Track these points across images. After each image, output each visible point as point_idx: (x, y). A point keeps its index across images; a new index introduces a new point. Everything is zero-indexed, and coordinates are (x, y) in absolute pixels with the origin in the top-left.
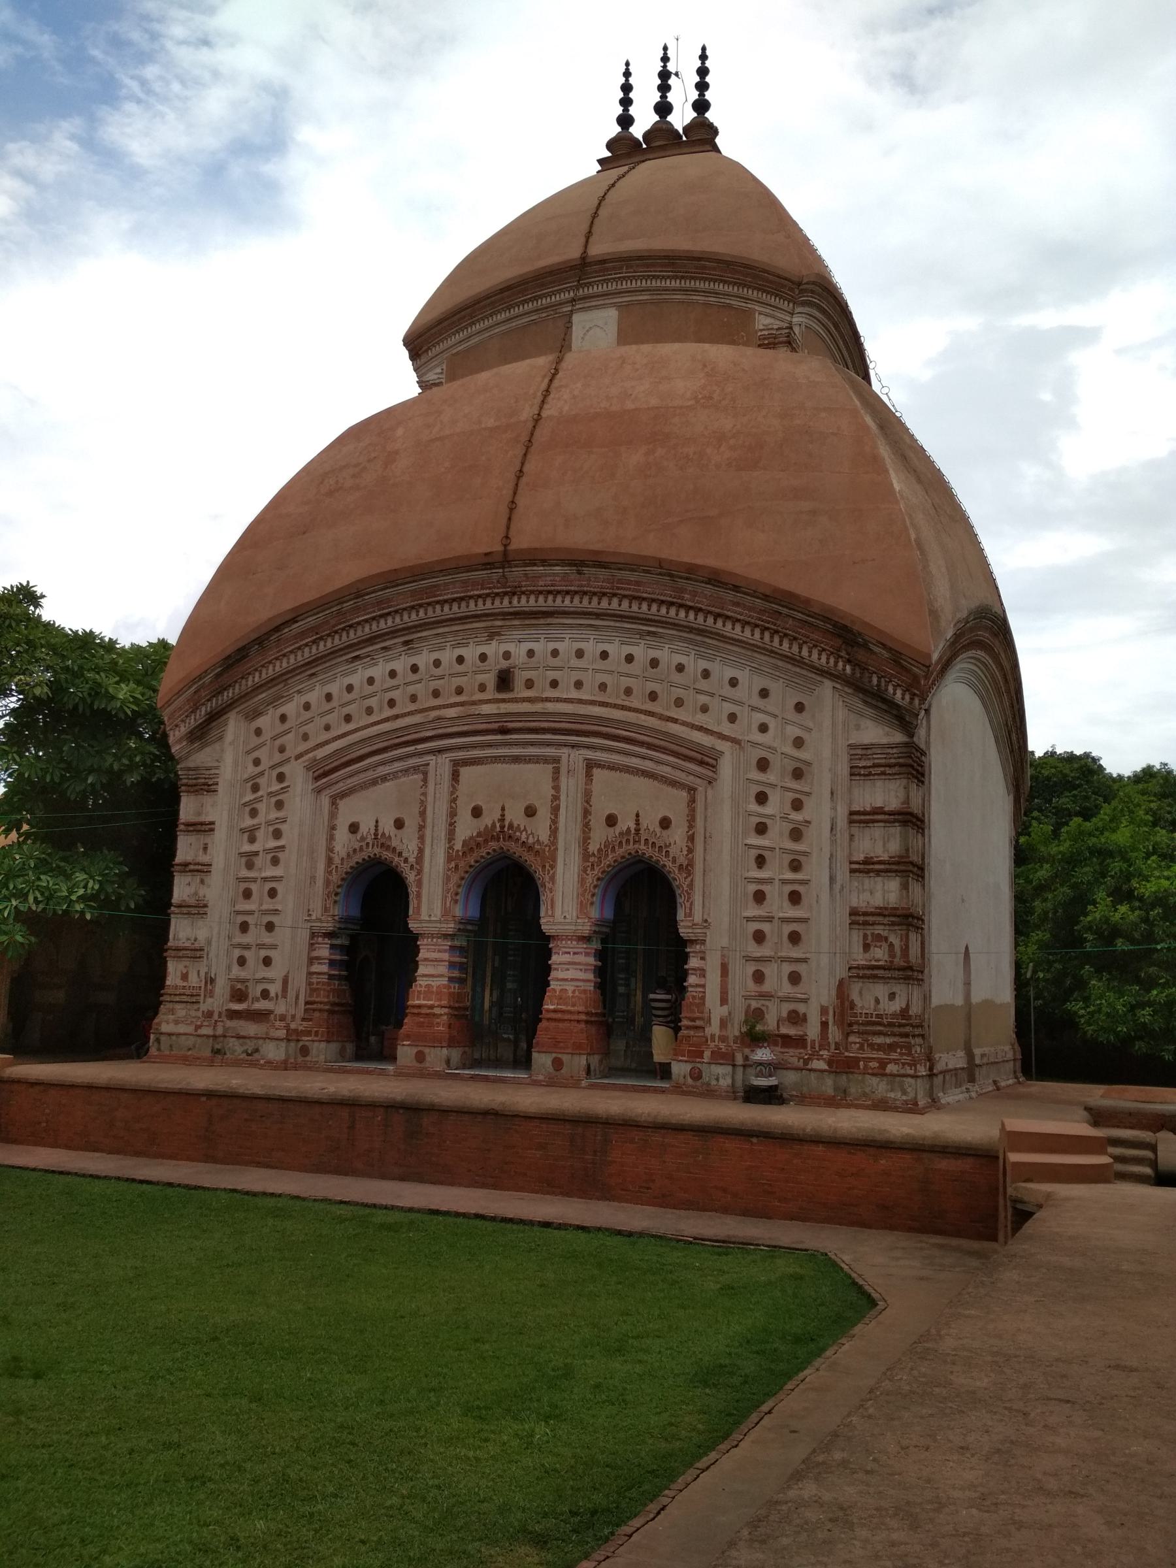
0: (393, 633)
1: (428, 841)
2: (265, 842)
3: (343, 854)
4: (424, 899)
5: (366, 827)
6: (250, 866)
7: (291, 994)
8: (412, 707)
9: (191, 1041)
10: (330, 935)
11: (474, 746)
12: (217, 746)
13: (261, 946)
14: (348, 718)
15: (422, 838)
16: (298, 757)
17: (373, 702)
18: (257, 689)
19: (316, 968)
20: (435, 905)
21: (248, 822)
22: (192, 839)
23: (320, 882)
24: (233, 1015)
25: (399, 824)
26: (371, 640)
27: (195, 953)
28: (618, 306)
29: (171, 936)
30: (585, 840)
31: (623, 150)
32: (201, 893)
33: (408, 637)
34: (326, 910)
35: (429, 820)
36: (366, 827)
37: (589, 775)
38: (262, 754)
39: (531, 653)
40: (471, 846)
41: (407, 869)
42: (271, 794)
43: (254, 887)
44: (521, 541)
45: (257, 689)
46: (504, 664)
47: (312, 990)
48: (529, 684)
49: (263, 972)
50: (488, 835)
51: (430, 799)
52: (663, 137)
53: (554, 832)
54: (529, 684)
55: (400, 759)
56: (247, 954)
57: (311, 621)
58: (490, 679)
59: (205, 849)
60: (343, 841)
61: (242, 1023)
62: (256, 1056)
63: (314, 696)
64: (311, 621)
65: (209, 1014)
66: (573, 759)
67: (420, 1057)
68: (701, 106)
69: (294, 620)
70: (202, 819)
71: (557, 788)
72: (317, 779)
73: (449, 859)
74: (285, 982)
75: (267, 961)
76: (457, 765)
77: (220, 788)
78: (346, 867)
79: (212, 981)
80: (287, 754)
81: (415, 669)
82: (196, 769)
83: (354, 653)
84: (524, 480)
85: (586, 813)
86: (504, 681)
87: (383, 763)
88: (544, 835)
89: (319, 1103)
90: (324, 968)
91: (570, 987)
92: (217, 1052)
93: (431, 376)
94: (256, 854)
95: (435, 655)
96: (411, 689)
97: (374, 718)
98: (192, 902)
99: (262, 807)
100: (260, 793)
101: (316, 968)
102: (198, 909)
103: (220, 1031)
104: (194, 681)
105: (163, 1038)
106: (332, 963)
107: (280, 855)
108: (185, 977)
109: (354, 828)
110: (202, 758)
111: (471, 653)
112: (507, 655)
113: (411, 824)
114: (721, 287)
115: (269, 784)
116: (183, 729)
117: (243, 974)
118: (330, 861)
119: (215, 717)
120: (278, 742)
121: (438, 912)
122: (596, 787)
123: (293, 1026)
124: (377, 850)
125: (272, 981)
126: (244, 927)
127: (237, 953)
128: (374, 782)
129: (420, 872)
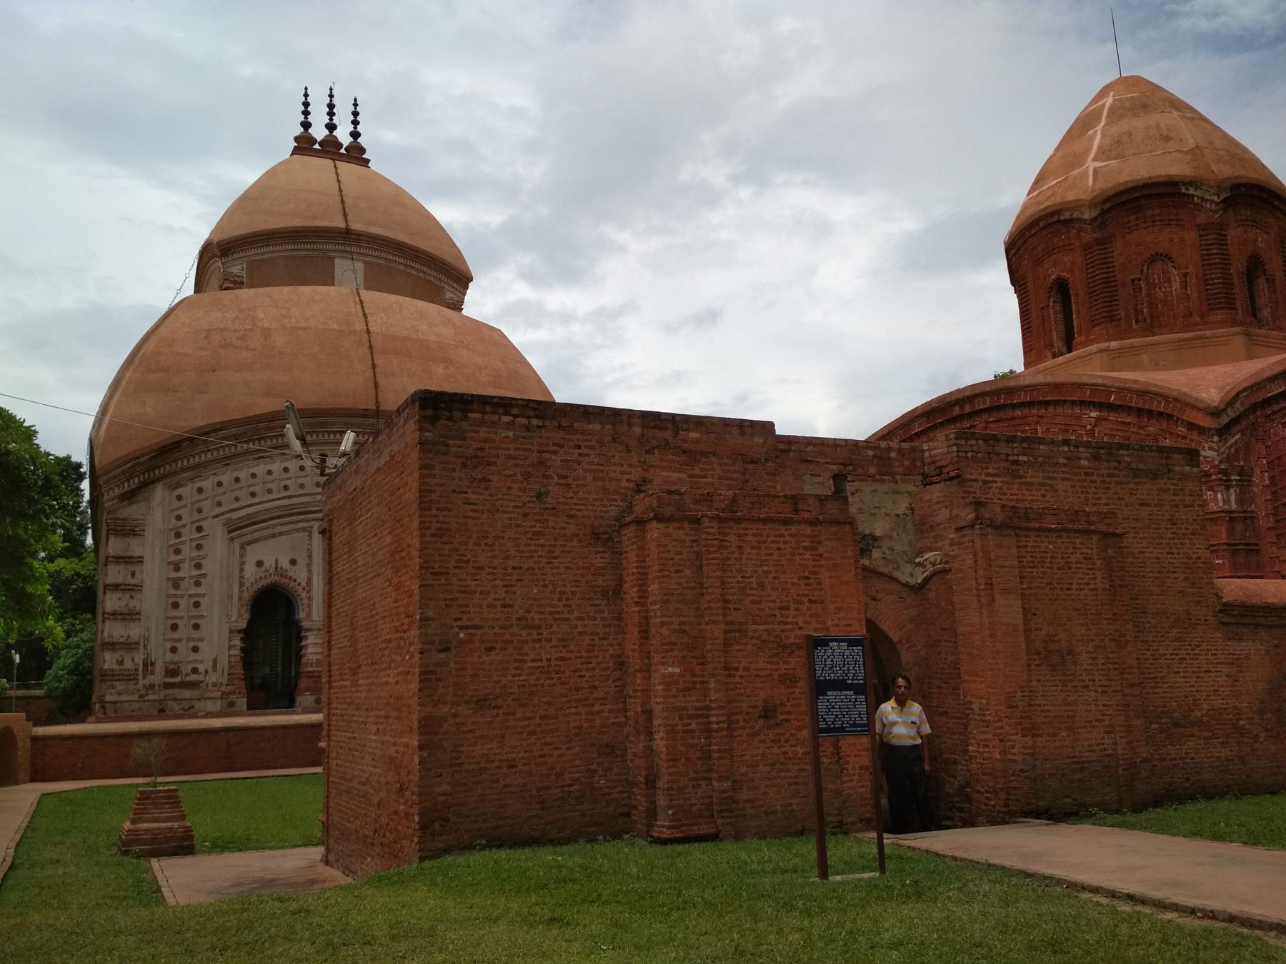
2: (187, 571)
3: (252, 580)
5: (269, 563)
6: (176, 586)
7: (219, 668)
9: (137, 705)
10: (239, 632)
14: (253, 495)
15: (310, 571)
16: (214, 517)
17: (272, 486)
18: (183, 470)
21: (173, 558)
22: (122, 567)
23: (236, 598)
24: (168, 686)
25: (293, 562)
27: (130, 646)
28: (364, 262)
29: (106, 635)
31: (304, 144)
34: (240, 615)
36: (269, 563)
38: (183, 512)
41: (299, 588)
42: (192, 540)
43: (181, 601)
45: (183, 470)
47: (231, 667)
49: (193, 656)
52: (330, 147)
55: (292, 523)
56: (177, 645)
57: (233, 431)
59: (133, 574)
60: (251, 572)
61: (177, 690)
62: (192, 711)
63: (226, 478)
65: (152, 686)
68: (355, 135)
69: (221, 429)
70: (130, 554)
72: (230, 532)
74: (215, 662)
75: (195, 649)
77: (149, 534)
78: (255, 588)
79: (152, 664)
80: (203, 515)
84: (377, 370)
87: (281, 525)
90: (238, 652)
92: (161, 711)
93: (235, 270)
94: (183, 579)
96: (301, 481)
98: (124, 610)
99: (186, 549)
100: (183, 539)
102: (130, 616)
103: (162, 696)
104: (131, 460)
105: (108, 706)
106: (242, 650)
107: (202, 580)
108: (121, 663)
110: (131, 511)
113: (302, 562)
114: (427, 270)
116: (116, 490)
117: (176, 658)
118: (241, 584)
119: (144, 485)
120: (196, 506)
123: (223, 689)
124: (277, 578)
125: (201, 662)
127: (169, 645)
128: (274, 536)
129: (309, 592)
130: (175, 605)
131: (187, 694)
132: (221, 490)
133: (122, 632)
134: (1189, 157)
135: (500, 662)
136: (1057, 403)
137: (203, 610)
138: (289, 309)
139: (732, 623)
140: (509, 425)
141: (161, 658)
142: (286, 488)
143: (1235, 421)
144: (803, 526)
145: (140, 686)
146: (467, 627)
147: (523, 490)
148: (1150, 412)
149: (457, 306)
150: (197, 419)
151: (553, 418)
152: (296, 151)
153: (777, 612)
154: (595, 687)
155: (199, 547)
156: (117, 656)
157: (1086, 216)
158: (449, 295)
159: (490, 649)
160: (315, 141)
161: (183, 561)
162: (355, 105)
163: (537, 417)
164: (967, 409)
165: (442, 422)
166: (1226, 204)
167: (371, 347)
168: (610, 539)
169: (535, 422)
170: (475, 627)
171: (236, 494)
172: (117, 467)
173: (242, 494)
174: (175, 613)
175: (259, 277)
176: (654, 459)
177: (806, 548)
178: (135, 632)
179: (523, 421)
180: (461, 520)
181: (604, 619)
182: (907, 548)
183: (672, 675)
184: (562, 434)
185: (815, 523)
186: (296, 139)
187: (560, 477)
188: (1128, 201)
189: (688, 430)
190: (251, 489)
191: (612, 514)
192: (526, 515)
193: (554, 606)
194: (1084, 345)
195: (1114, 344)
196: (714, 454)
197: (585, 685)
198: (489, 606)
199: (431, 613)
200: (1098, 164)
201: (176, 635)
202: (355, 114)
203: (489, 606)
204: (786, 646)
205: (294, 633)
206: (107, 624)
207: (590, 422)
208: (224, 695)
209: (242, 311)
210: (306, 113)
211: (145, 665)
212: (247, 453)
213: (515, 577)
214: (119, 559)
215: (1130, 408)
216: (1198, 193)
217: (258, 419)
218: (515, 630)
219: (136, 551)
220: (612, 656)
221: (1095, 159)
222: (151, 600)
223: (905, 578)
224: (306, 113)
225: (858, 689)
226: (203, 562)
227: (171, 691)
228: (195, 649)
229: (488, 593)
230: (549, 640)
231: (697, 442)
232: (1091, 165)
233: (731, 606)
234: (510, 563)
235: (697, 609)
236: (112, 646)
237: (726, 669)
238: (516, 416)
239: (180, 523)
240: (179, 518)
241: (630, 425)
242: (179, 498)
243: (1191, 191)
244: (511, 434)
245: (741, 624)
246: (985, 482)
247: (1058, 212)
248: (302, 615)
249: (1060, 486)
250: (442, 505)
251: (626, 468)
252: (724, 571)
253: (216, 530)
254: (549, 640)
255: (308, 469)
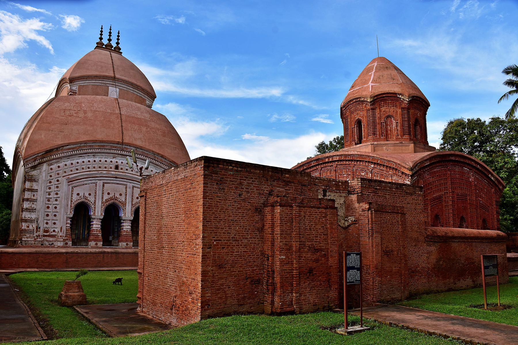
0: (91, 153)
1: (97, 199)
2: (53, 195)
4: (96, 211)
5: (81, 194)
6: (49, 201)
7: (63, 231)
8: (94, 169)
10: (70, 218)
11: (108, 180)
12: (38, 171)
13: (53, 220)
14: (77, 169)
15: (95, 198)
16: (63, 177)
17: (84, 167)
18: (53, 159)
19: (67, 225)
20: (98, 213)
21: (49, 190)
23: (69, 206)
24: (44, 236)
25: (90, 194)
26: (86, 153)
27: (31, 221)
28: (119, 89)
30: (132, 201)
31: (100, 45)
32: (33, 206)
33: (94, 154)
34: (71, 212)
35: (97, 194)
37: (133, 188)
39: (122, 163)
40: (107, 201)
44: (126, 141)
45: (53, 159)
46: (117, 164)
47: (66, 230)
48: (122, 169)
50: (111, 199)
51: (97, 189)
52: (109, 47)
53: (126, 199)
54: (122, 169)
56: (48, 221)
57: (72, 146)
58: (113, 167)
59: (34, 196)
63: (68, 163)
64: (72, 146)
65: (39, 236)
66: (130, 185)
67: (96, 244)
68: (118, 43)
70: (33, 188)
71: (126, 191)
72: (68, 182)
73: (102, 203)
74: (61, 228)
75: (55, 223)
76: (104, 183)
77: (40, 181)
78: (76, 203)
79: (39, 228)
80: (59, 176)
81: (95, 161)
82: (32, 176)
83: (80, 155)
85: (132, 196)
86: (117, 167)
88: (124, 200)
89: (96, 253)
90: (69, 225)
91: (128, 230)
93: (74, 88)
95: (100, 159)
96: (94, 165)
97: (84, 171)
98: (30, 208)
101: (67, 225)
102: (31, 210)
106: (71, 224)
108: (28, 227)
109: (78, 194)
110: (34, 173)
111: (109, 160)
112: (117, 162)
113: (93, 195)
115: (54, 182)
117: (47, 226)
118: (71, 201)
119: (40, 164)
121: (100, 214)
122: (134, 191)
124: (84, 200)
126: (48, 215)
127: (45, 221)
128: (83, 185)
130: (48, 207)
131: (51, 239)
132: (66, 167)
133: (29, 216)
134: (400, 86)
135: (226, 253)
136: (360, 161)
137: (58, 210)
138: (93, 104)
139: (301, 242)
140: (231, 170)
141: (43, 226)
142: (89, 168)
143: (416, 173)
144: (322, 209)
145: (35, 236)
146: (217, 240)
147: (234, 193)
148: (378, 164)
149: (150, 107)
150: (59, 142)
151: (245, 168)
152: (97, 47)
153: (314, 238)
154: (254, 261)
155: (57, 187)
156: (27, 224)
157: (369, 100)
158: (147, 102)
159: (223, 248)
160: (104, 44)
161: (52, 192)
162: (119, 33)
163: (240, 167)
164: (331, 160)
165: (211, 168)
166: (410, 102)
167: (121, 119)
168: (261, 211)
169: (239, 169)
170: (219, 240)
171: (71, 169)
172: (30, 157)
173: (73, 169)
174: (48, 210)
175: (82, 91)
176: (275, 183)
177: (323, 217)
178: (33, 216)
179: (236, 168)
180: (216, 203)
181: (258, 238)
182: (343, 215)
183: (282, 259)
184: (247, 174)
185: (326, 208)
186: (97, 43)
187: (246, 189)
188: (381, 97)
189: (286, 174)
190: (77, 167)
191: (262, 202)
192: (235, 201)
193: (243, 234)
194: (366, 142)
195: (375, 143)
196: (293, 182)
197: (252, 261)
198: (223, 233)
199: (206, 235)
200: (373, 84)
201: (48, 218)
202: (118, 36)
203: (223, 233)
204: (316, 250)
205: (89, 220)
206: (24, 213)
207: (256, 170)
208: (64, 240)
209: (77, 103)
210: (101, 35)
211: (37, 228)
212: (76, 155)
213: (232, 223)
214: (29, 190)
215: (384, 165)
216: (402, 97)
217: (81, 143)
218: (231, 241)
219: (35, 187)
220: (260, 251)
221: (372, 83)
222: (39, 205)
223: (342, 225)
224: (101, 35)
225: (358, 269)
226: (58, 192)
227: (45, 238)
228: (55, 223)
229: (223, 228)
230: (241, 245)
231: (288, 178)
232: (370, 84)
233: (301, 236)
234: (230, 218)
235: (291, 237)
236: (26, 221)
237: (299, 257)
238: (233, 167)
239: (51, 178)
240: (51, 176)
241: (268, 171)
242: (51, 169)
243: (400, 96)
244: (232, 173)
245: (304, 242)
246: (368, 195)
247: (360, 98)
248: (92, 213)
249: (387, 196)
250: (210, 197)
251: (266, 186)
252: (300, 224)
253: (64, 181)
254: (241, 245)
255: (97, 161)
